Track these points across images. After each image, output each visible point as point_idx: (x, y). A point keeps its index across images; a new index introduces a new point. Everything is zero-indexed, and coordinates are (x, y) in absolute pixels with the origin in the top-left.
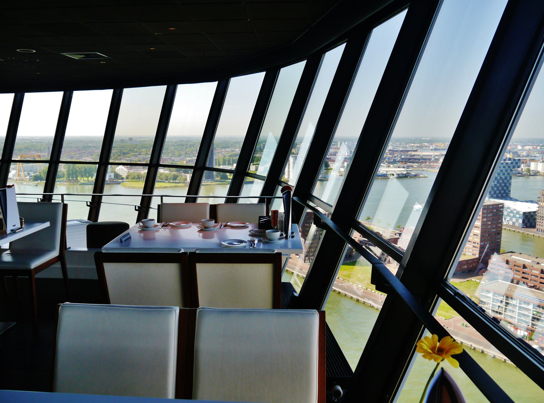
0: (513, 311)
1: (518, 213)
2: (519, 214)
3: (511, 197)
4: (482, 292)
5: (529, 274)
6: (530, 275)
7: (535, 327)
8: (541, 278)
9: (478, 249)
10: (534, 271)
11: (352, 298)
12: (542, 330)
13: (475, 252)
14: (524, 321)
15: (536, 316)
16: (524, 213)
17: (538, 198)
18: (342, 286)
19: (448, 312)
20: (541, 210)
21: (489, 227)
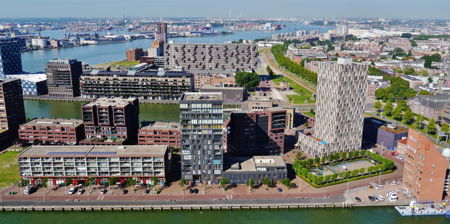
0: (49, 168)
1: (32, 84)
2: (33, 85)
4: (20, 161)
6: (54, 133)
7: (68, 174)
8: (63, 134)
9: (7, 123)
10: (56, 130)
12: (74, 175)
13: (4, 126)
16: (37, 83)
17: (45, 69)
21: (12, 101)
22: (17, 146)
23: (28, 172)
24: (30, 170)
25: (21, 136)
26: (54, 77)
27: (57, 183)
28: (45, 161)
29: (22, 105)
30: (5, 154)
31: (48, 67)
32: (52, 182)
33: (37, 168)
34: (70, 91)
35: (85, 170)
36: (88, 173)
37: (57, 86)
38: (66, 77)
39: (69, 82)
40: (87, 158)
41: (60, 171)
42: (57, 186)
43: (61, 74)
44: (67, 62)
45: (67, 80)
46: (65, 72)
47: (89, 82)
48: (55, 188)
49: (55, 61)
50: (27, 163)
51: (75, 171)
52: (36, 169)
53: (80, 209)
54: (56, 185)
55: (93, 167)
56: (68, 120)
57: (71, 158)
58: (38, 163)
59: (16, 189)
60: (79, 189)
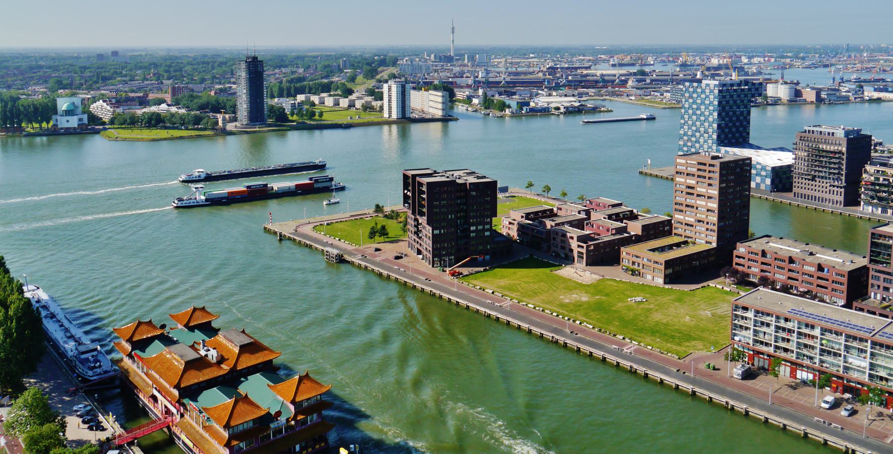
0: (788, 340)
1: (764, 168)
2: (766, 170)
3: (750, 142)
4: (736, 311)
5: (798, 273)
7: (824, 365)
8: (819, 278)
9: (715, 234)
10: (806, 267)
11: (519, 327)
12: (837, 371)
13: (709, 239)
14: (807, 356)
15: (826, 347)
16: (773, 168)
17: (794, 144)
18: (501, 306)
19: (681, 345)
20: (800, 164)
22: (728, 280)
23: (746, 337)
24: (749, 334)
25: (737, 264)
26: (808, 161)
27: (799, 376)
28: (782, 324)
29: (746, 206)
30: (706, 290)
31: (800, 140)
32: (788, 369)
33: (765, 333)
34: (839, 193)
35: (864, 368)
36: (871, 376)
37: (813, 179)
38: (835, 163)
39: (838, 173)
40: (874, 344)
41: (808, 354)
42: (798, 381)
43: (823, 157)
44: (840, 133)
45: (834, 169)
46: (835, 153)
47: (884, 180)
48: (793, 384)
49: (815, 129)
50: (746, 318)
51: (842, 364)
52: (761, 335)
53: (844, 449)
54: (796, 378)
55: (885, 368)
56: (832, 252)
57: (837, 333)
58: (768, 325)
59: (720, 362)
60: (845, 403)
